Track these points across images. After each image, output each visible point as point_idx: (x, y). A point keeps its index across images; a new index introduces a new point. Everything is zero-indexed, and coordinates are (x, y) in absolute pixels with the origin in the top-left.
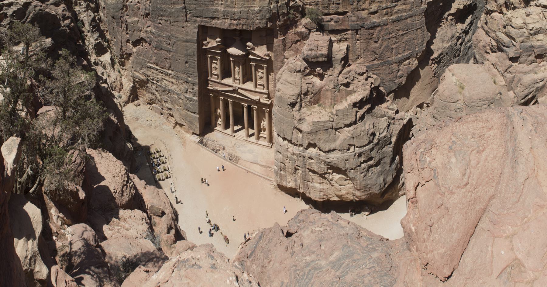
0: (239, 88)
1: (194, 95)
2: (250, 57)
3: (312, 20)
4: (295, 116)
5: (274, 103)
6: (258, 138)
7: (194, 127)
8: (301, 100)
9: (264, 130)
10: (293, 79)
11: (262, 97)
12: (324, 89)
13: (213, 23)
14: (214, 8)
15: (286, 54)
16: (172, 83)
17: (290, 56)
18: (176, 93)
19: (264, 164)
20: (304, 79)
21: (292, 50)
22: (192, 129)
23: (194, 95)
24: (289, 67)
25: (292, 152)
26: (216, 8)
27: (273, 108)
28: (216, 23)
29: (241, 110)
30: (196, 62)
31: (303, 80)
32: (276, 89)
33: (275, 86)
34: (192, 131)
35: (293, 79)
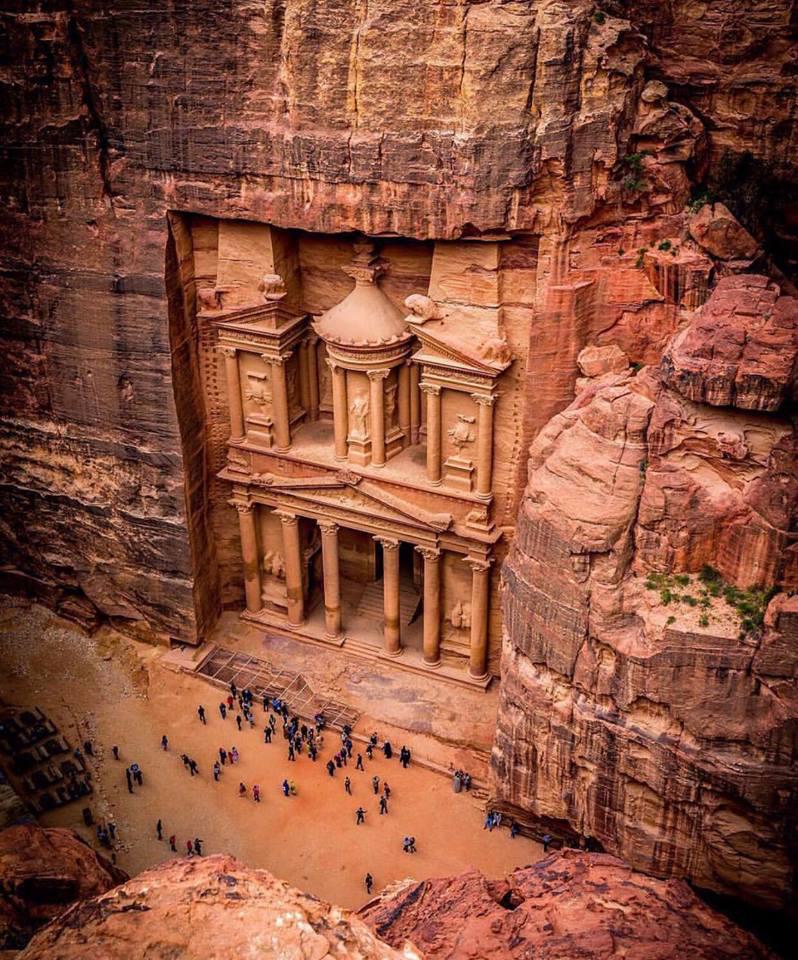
0: (364, 477)
1: (169, 507)
2: (420, 356)
3: (738, 210)
4: (595, 597)
5: (515, 540)
6: (437, 655)
7: (174, 622)
8: (632, 546)
9: (464, 630)
10: (604, 460)
11: (462, 517)
12: (740, 521)
13: (242, 202)
14: (242, 125)
15: (588, 358)
16: (64, 470)
17: (606, 368)
18: (90, 510)
19: (456, 736)
20: (657, 469)
21: (619, 343)
22: (167, 629)
23: (169, 507)
24: (596, 411)
25: (567, 712)
26: (256, 125)
27: (507, 558)
28: (257, 203)
29: (372, 559)
30: (168, 380)
31: (650, 472)
32: (527, 491)
33: (523, 480)
34: (167, 638)
35: (604, 460)
